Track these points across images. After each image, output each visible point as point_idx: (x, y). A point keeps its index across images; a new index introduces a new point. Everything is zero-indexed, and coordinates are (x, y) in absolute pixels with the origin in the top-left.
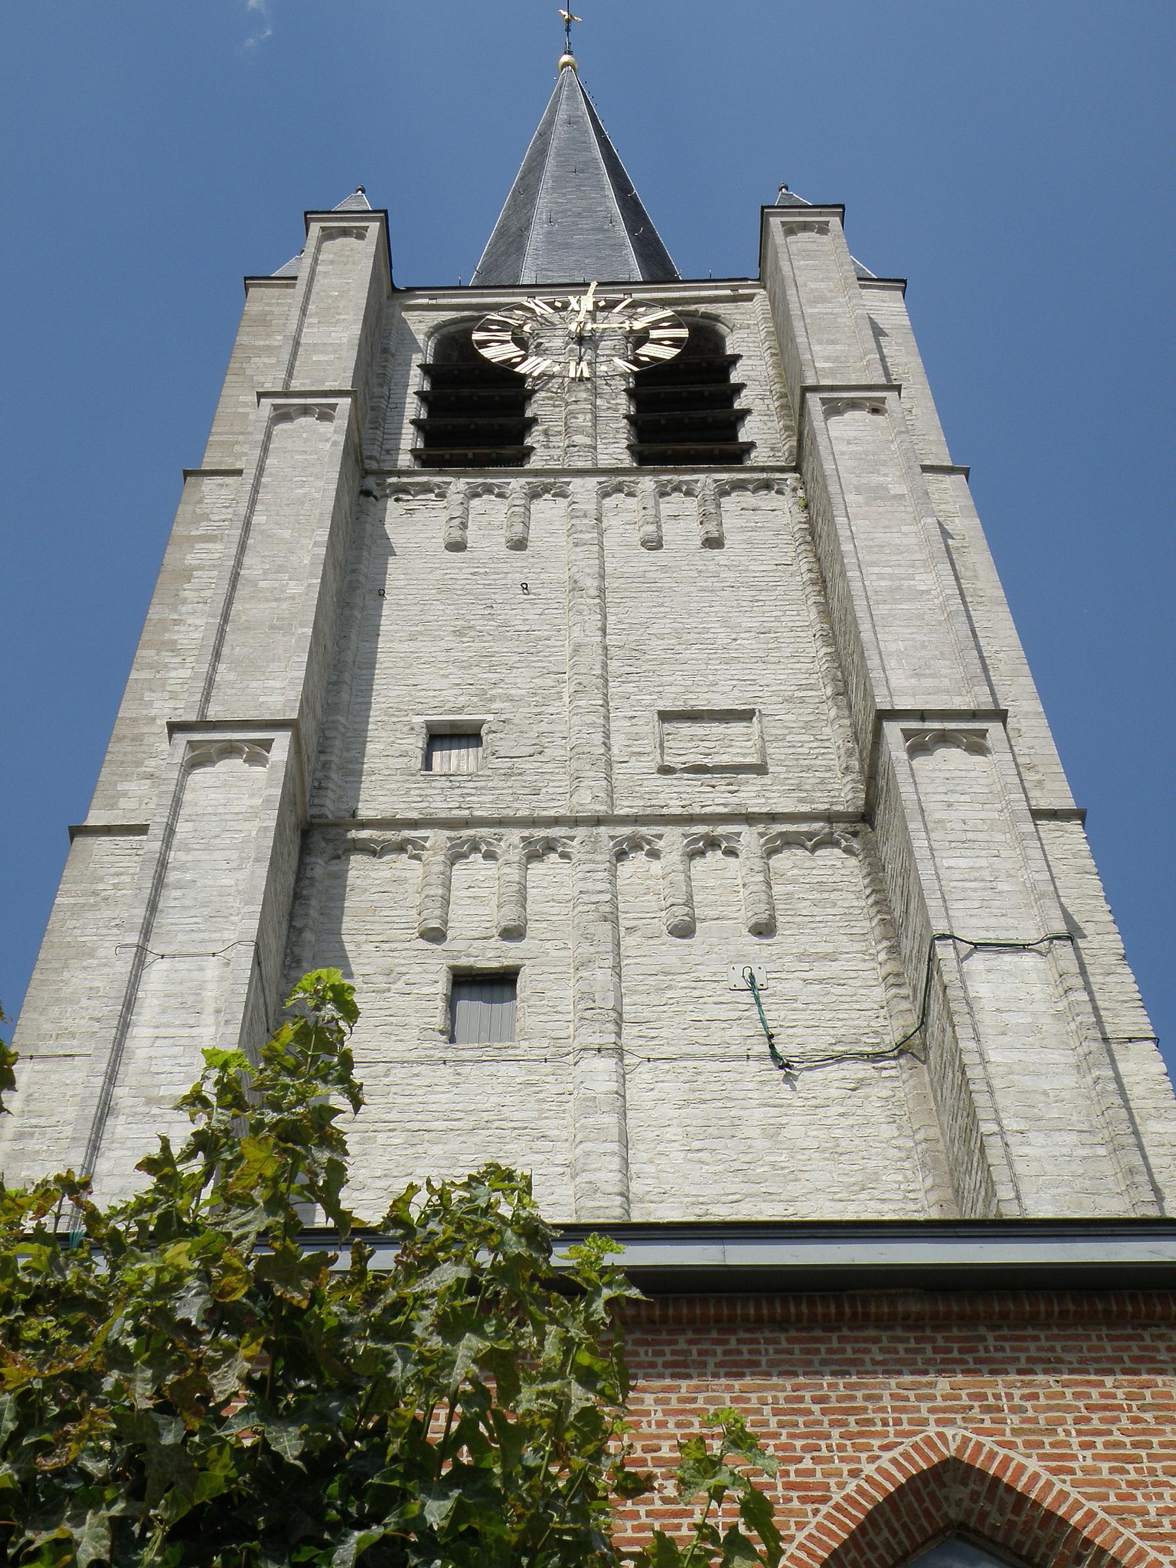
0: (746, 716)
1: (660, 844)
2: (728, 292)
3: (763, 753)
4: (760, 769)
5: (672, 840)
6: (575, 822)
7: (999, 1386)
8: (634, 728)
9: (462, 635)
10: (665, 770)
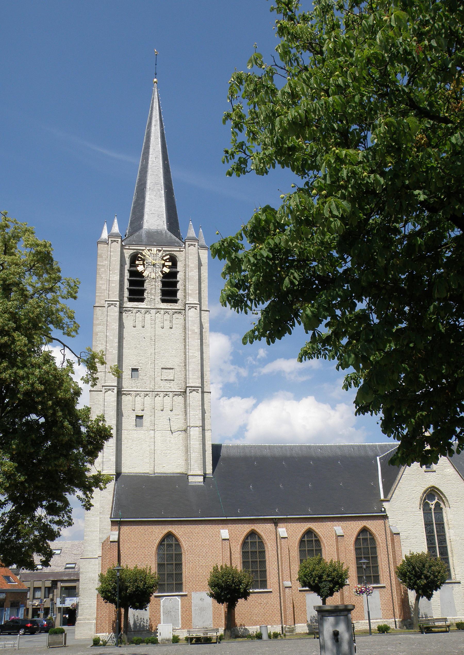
0: (173, 369)
1: (160, 395)
2: (178, 249)
3: (174, 377)
4: (174, 380)
5: (162, 394)
6: (150, 391)
7: (173, 526)
8: (158, 370)
10: (162, 380)
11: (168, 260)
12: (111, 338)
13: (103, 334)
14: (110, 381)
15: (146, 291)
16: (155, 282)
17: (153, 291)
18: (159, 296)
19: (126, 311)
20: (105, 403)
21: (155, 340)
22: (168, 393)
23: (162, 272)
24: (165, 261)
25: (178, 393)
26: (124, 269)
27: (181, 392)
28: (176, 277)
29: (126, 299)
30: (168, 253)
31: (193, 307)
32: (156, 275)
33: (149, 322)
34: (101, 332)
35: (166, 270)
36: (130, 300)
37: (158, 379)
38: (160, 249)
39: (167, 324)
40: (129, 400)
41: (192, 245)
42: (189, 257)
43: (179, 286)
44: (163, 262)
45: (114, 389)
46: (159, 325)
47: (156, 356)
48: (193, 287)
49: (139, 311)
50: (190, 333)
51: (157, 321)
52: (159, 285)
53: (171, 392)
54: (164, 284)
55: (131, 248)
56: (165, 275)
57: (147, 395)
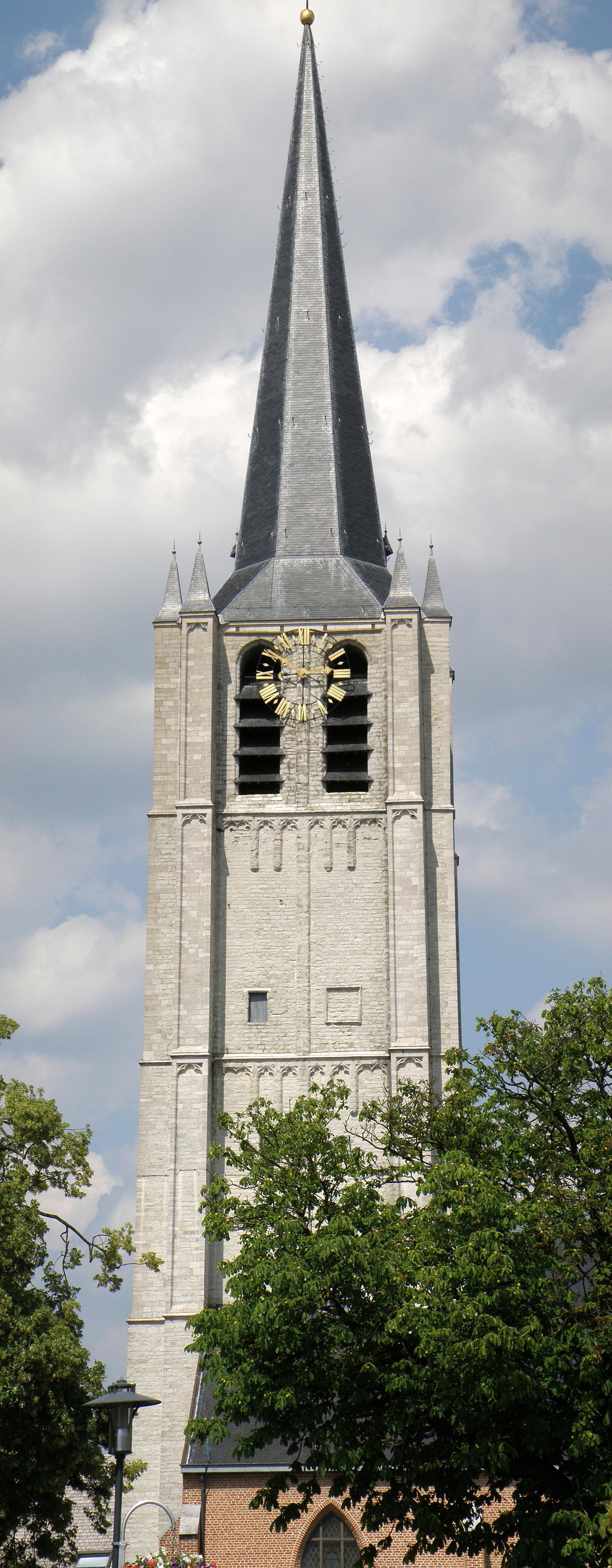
0: (357, 989)
1: (325, 1070)
2: (369, 627)
3: (361, 1013)
4: (359, 1024)
9: (259, 934)
10: (328, 1024)
11: (341, 663)
12: (194, 914)
13: (172, 896)
14: (192, 1041)
15: (285, 761)
16: (308, 732)
17: (303, 761)
18: (318, 773)
19: (232, 823)
20: (180, 1106)
21: (309, 907)
22: (344, 1063)
23: (325, 698)
24: (334, 665)
25: (370, 1062)
26: (226, 695)
27: (379, 1058)
28: (364, 711)
29: (231, 788)
30: (339, 638)
31: (405, 812)
32: (309, 712)
33: (294, 853)
34: (167, 891)
35: (337, 693)
36: (245, 789)
37: (318, 1021)
38: (320, 628)
39: (341, 857)
40: (243, 1086)
41: (402, 621)
42: (396, 659)
43: (373, 738)
44: (328, 670)
45: (201, 1064)
46: (319, 860)
47: (313, 954)
48: (406, 748)
49: (266, 823)
50: (398, 889)
51: (314, 849)
52: (319, 738)
53: (353, 1058)
54: (333, 734)
55: (242, 630)
56: (334, 708)
57: (290, 1069)
